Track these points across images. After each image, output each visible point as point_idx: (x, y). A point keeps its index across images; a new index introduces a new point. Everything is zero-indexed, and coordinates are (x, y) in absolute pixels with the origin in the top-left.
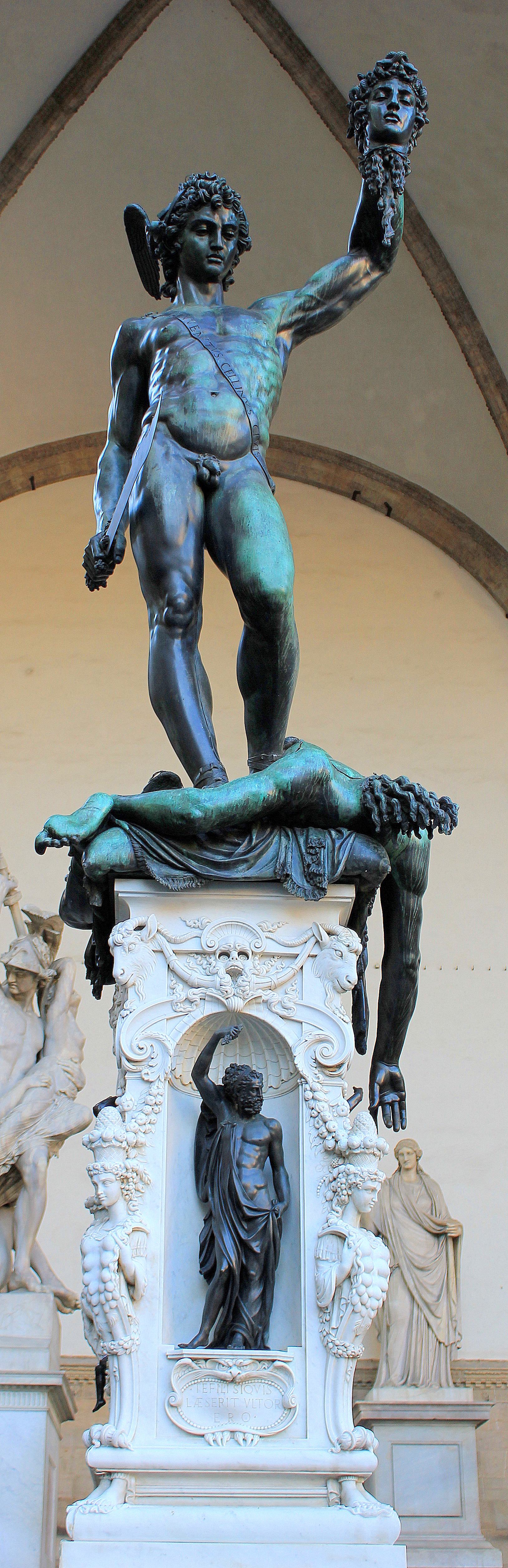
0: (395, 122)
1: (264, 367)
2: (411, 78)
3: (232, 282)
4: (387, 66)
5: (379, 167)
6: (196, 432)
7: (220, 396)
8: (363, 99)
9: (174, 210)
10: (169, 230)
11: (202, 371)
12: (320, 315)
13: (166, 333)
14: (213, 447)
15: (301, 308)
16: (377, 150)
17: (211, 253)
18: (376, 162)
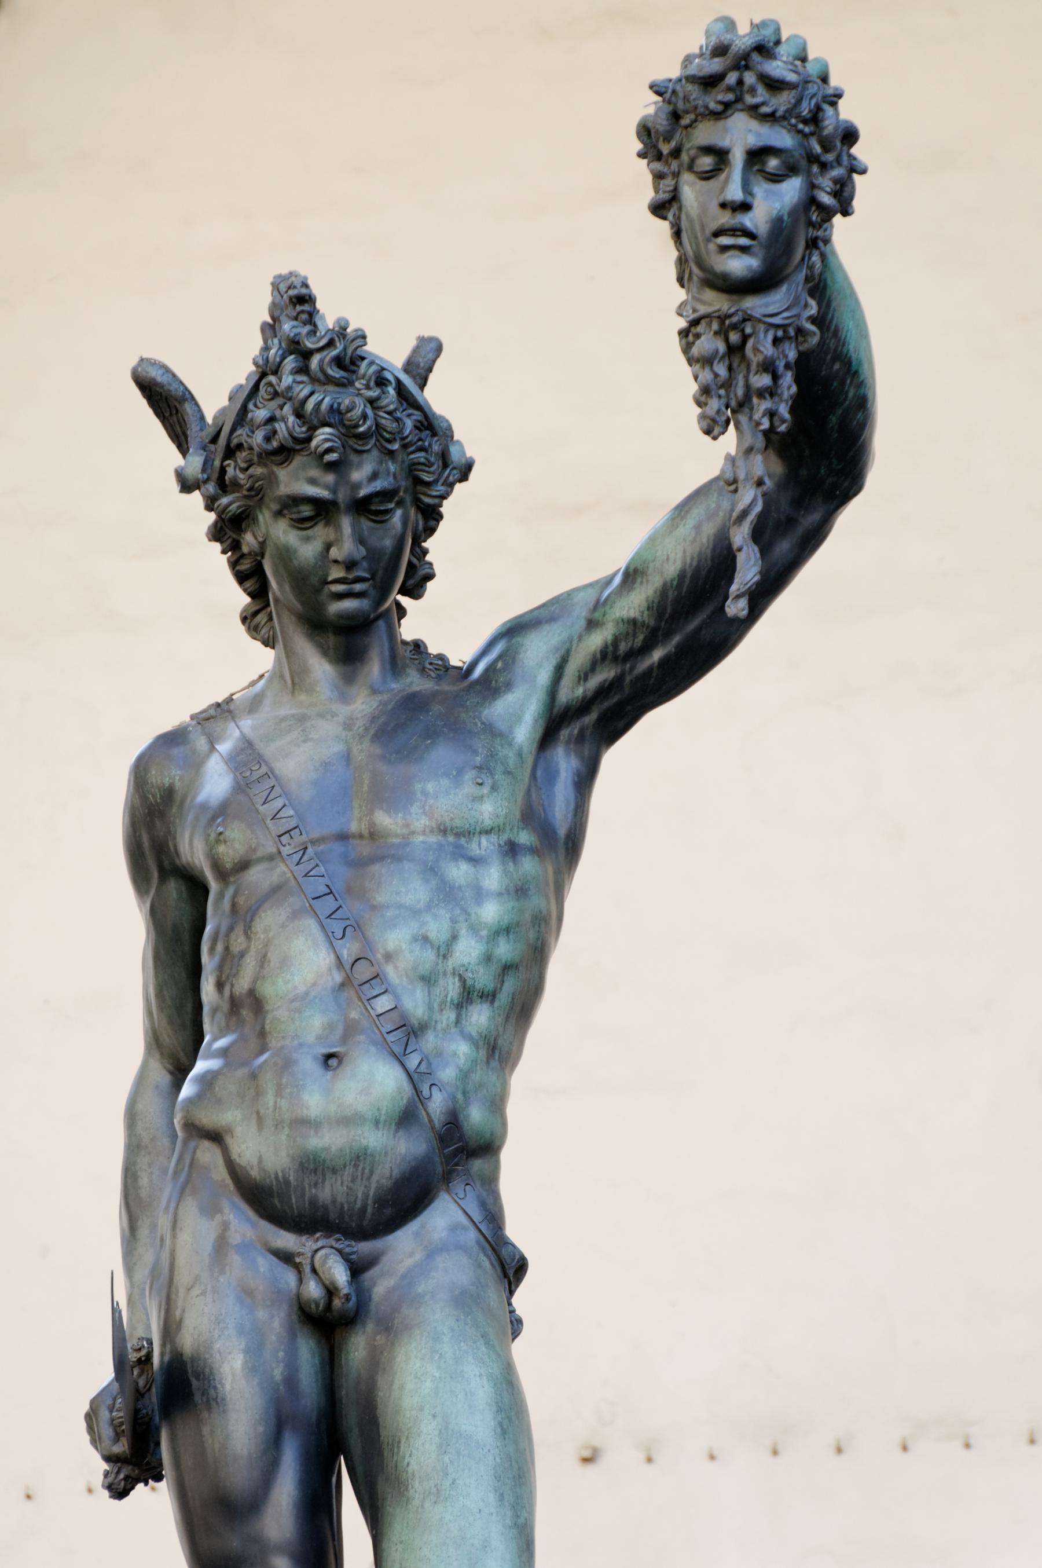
1: (474, 929)
3: (430, 577)
4: (709, 82)
6: (287, 1182)
7: (347, 1070)
11: (302, 989)
12: (664, 662)
14: (333, 1216)
15: (606, 655)
17: (336, 573)
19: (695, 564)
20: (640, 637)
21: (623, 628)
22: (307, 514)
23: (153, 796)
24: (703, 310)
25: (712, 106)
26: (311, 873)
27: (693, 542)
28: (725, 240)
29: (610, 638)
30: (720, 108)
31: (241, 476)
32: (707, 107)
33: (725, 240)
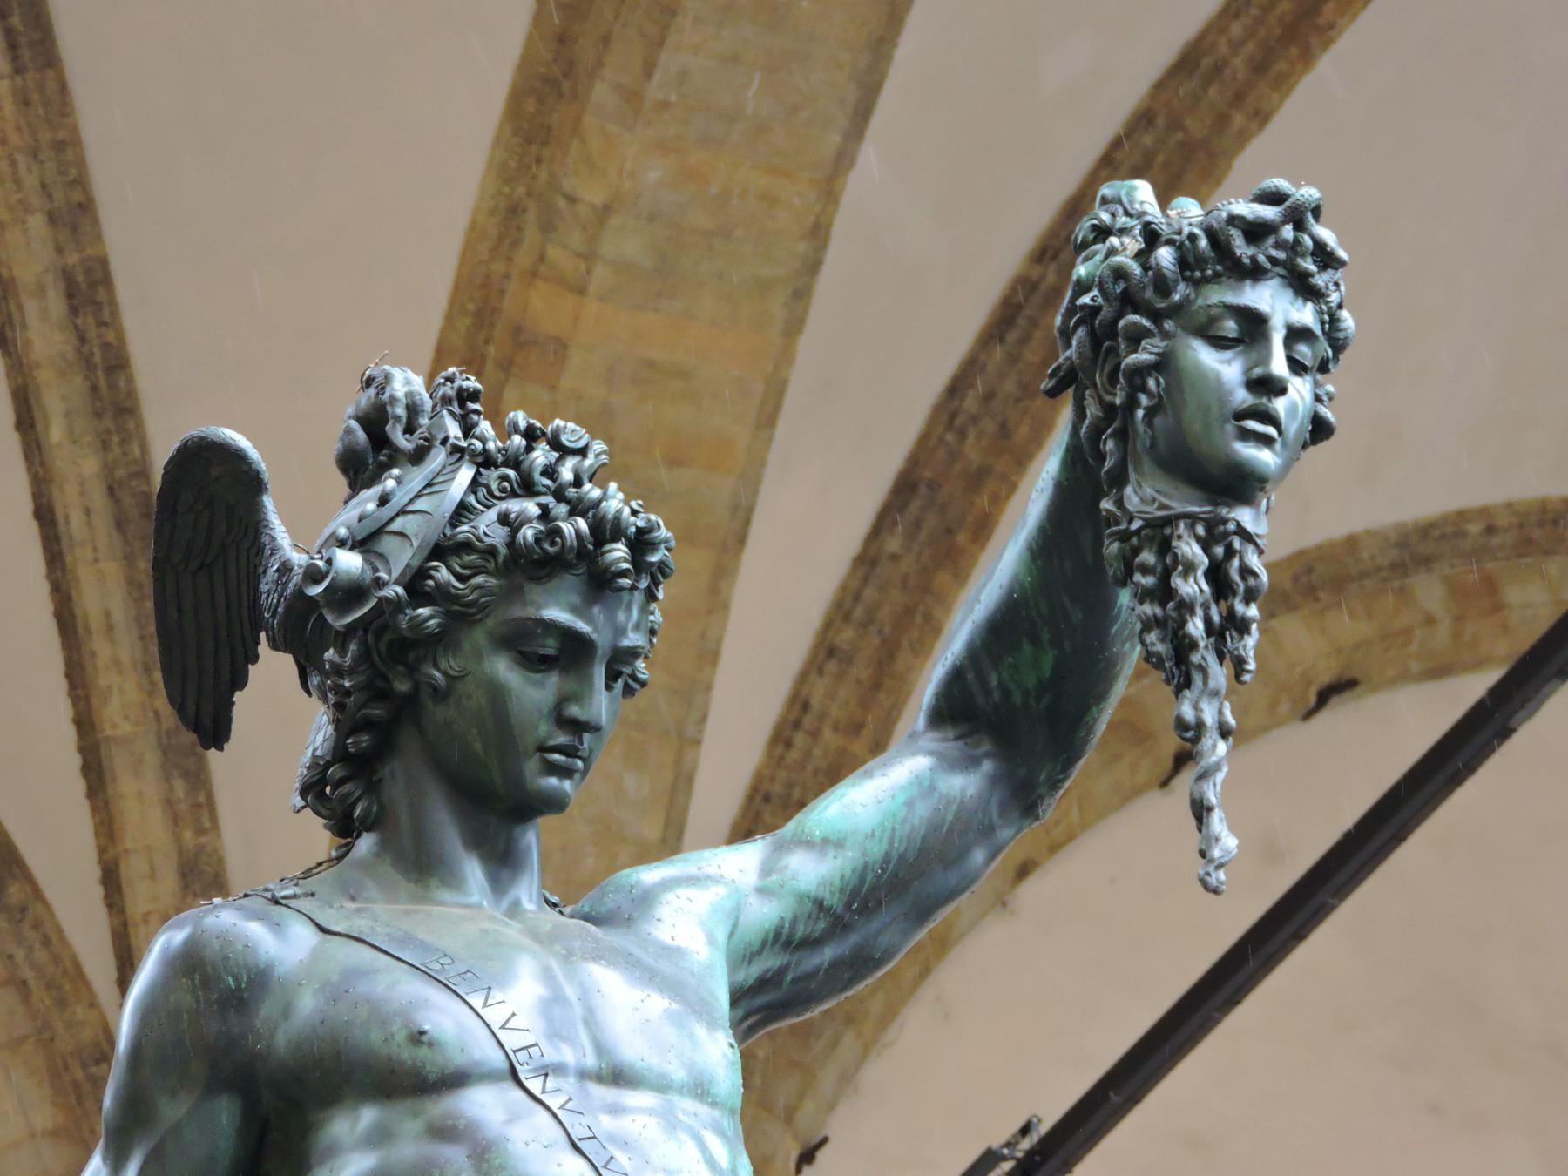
0: (1266, 441)
2: (1320, 280)
4: (1256, 231)
5: (1193, 587)
8: (1156, 316)
9: (440, 551)
10: (417, 624)
12: (835, 965)
13: (423, 1052)
15: (782, 939)
16: (1192, 519)
17: (562, 739)
18: (1189, 568)
19: (902, 849)
20: (822, 925)
21: (808, 907)
22: (550, 651)
23: (236, 979)
24: (1179, 507)
25: (1261, 258)
26: (568, 1106)
27: (904, 821)
28: (1252, 424)
29: (789, 916)
30: (1268, 265)
31: (457, 584)
32: (1253, 259)
33: (1252, 424)
